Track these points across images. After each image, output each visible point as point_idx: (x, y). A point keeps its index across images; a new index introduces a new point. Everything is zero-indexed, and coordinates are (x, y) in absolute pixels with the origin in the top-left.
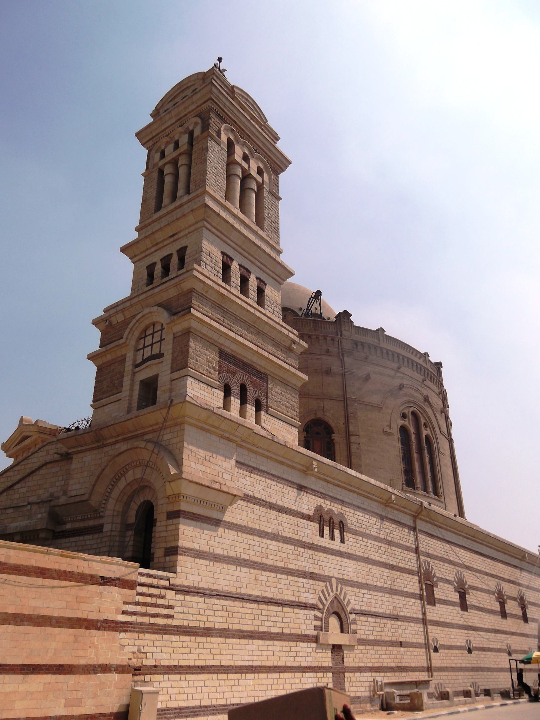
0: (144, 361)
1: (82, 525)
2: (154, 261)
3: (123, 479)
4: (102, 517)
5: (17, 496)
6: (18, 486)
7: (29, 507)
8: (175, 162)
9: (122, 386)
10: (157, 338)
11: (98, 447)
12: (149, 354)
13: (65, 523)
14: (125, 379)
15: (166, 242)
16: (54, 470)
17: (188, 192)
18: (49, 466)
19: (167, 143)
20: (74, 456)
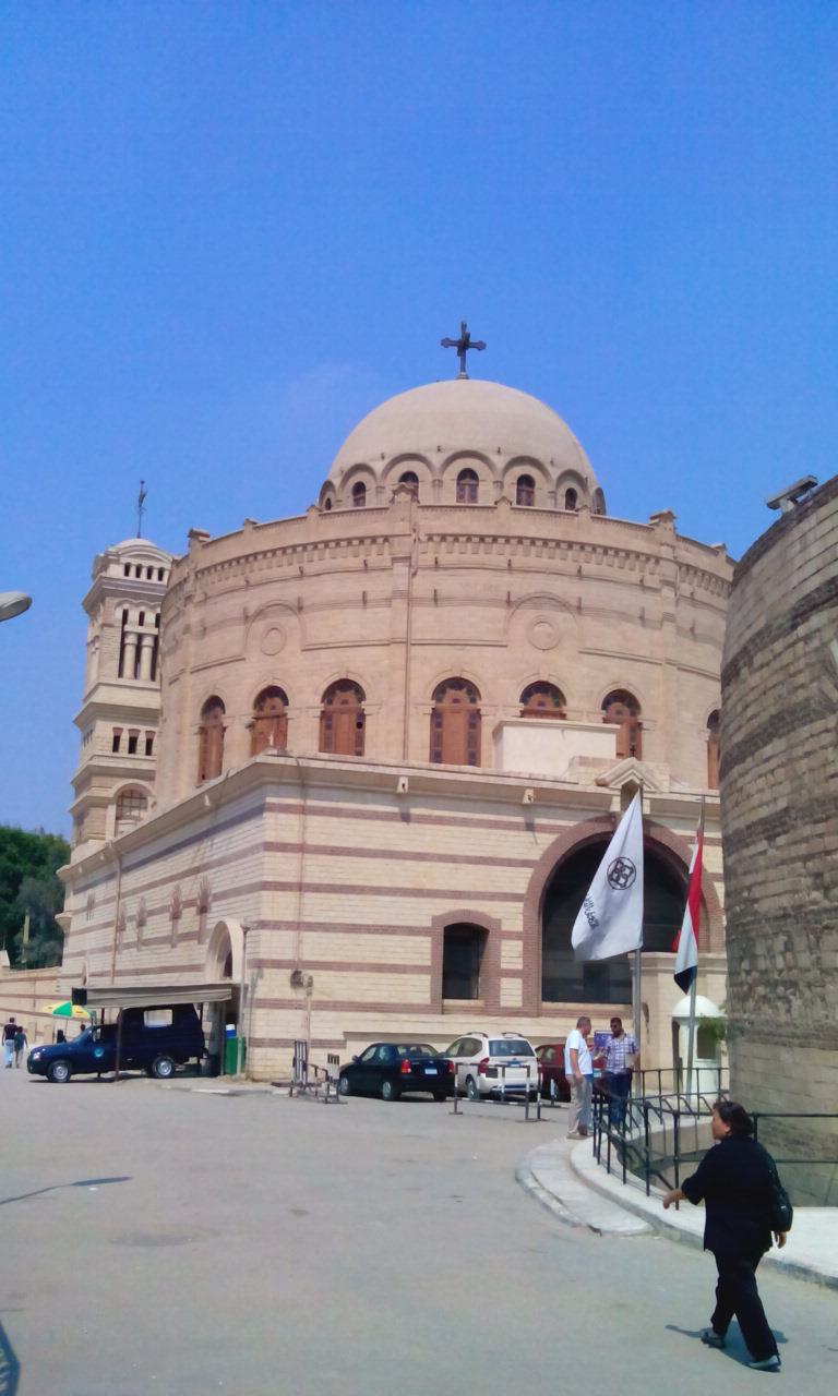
8: (140, 637)
17: (153, 677)
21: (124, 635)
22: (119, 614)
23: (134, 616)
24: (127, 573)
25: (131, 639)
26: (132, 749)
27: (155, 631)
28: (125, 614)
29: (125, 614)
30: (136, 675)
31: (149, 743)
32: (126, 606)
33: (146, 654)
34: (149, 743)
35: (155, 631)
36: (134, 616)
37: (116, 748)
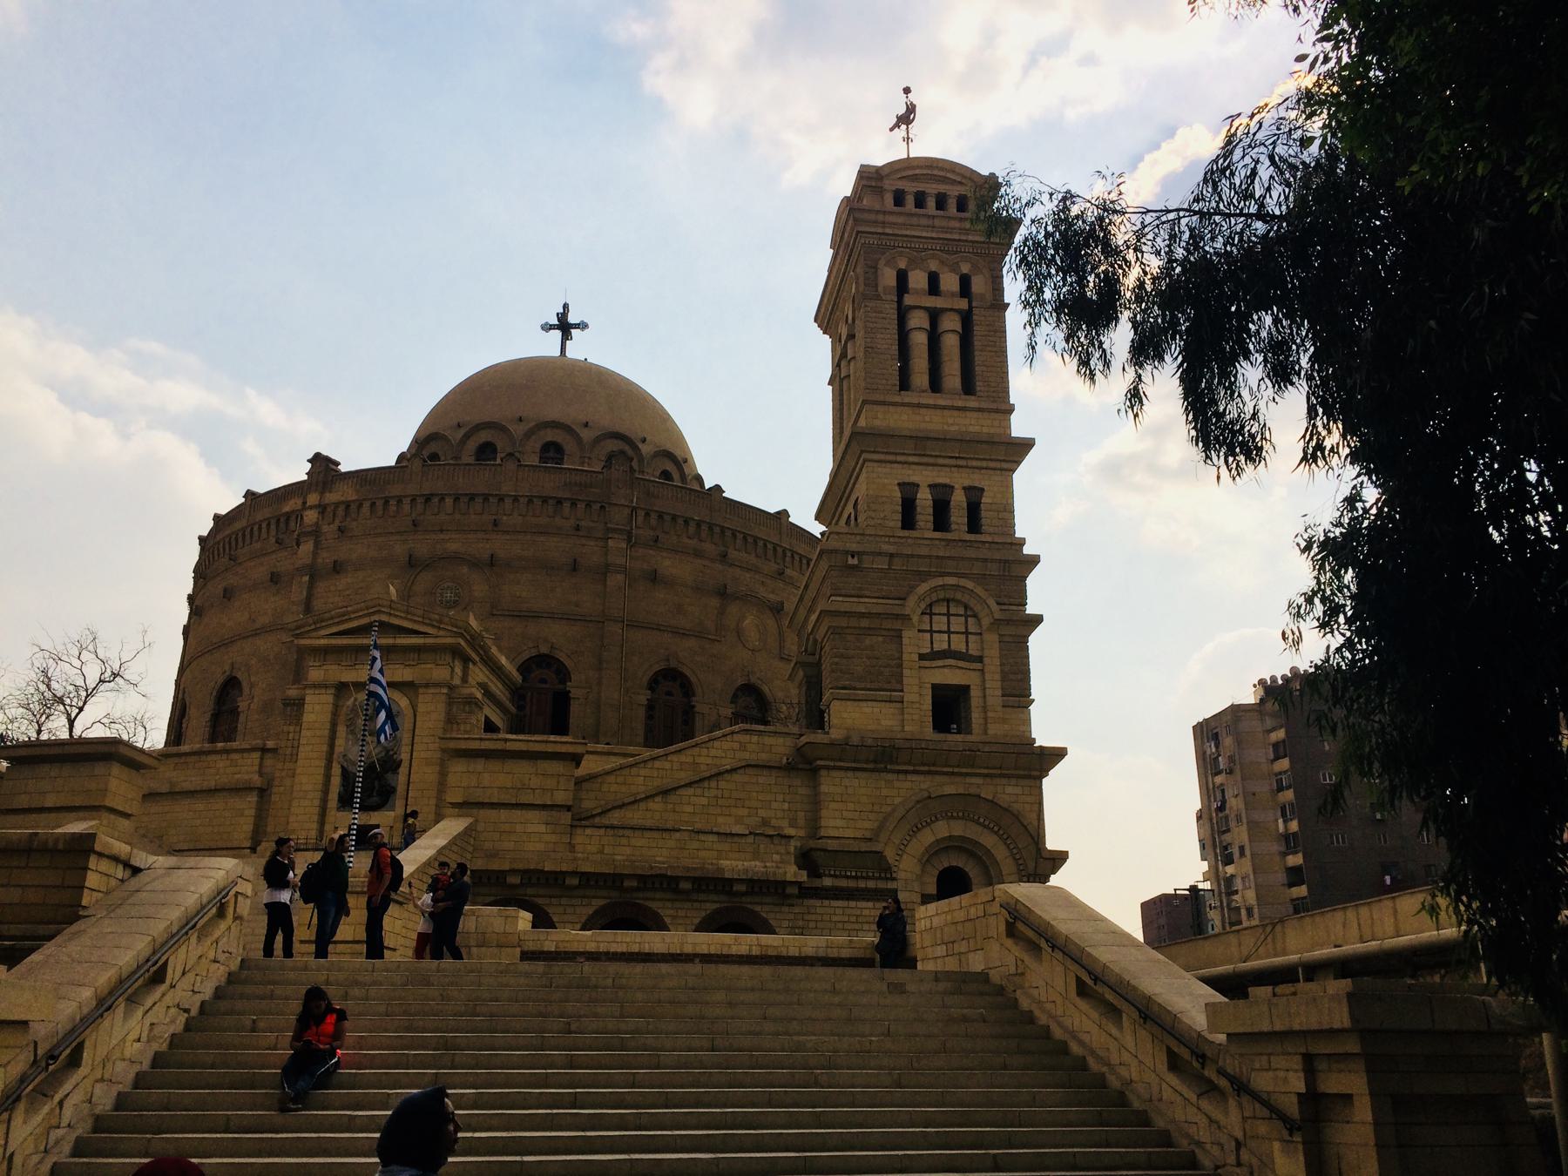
0: (935, 655)
1: (851, 884)
2: (914, 479)
3: (927, 831)
4: (894, 879)
5: (689, 809)
6: (690, 791)
7: (750, 839)
9: (901, 682)
10: (957, 624)
11: (872, 770)
12: (945, 646)
13: (819, 876)
14: (906, 672)
15: (941, 461)
16: (761, 780)
17: (968, 387)
18: (748, 771)
19: (913, 263)
20: (823, 772)
21: (902, 314)
22: (889, 278)
23: (918, 280)
24: (899, 199)
25: (918, 320)
26: (941, 519)
27: (963, 304)
28: (902, 277)
29: (902, 277)
30: (935, 385)
31: (974, 510)
32: (902, 265)
33: (951, 343)
34: (974, 510)
35: (963, 304)
36: (918, 280)
37: (908, 521)
